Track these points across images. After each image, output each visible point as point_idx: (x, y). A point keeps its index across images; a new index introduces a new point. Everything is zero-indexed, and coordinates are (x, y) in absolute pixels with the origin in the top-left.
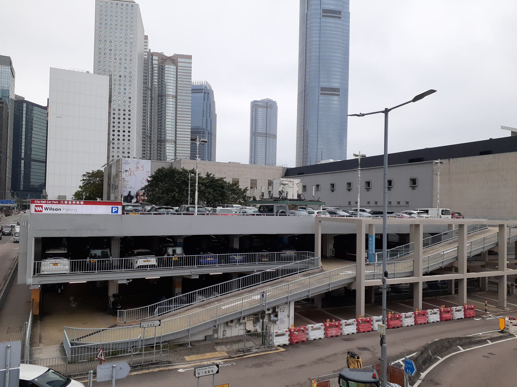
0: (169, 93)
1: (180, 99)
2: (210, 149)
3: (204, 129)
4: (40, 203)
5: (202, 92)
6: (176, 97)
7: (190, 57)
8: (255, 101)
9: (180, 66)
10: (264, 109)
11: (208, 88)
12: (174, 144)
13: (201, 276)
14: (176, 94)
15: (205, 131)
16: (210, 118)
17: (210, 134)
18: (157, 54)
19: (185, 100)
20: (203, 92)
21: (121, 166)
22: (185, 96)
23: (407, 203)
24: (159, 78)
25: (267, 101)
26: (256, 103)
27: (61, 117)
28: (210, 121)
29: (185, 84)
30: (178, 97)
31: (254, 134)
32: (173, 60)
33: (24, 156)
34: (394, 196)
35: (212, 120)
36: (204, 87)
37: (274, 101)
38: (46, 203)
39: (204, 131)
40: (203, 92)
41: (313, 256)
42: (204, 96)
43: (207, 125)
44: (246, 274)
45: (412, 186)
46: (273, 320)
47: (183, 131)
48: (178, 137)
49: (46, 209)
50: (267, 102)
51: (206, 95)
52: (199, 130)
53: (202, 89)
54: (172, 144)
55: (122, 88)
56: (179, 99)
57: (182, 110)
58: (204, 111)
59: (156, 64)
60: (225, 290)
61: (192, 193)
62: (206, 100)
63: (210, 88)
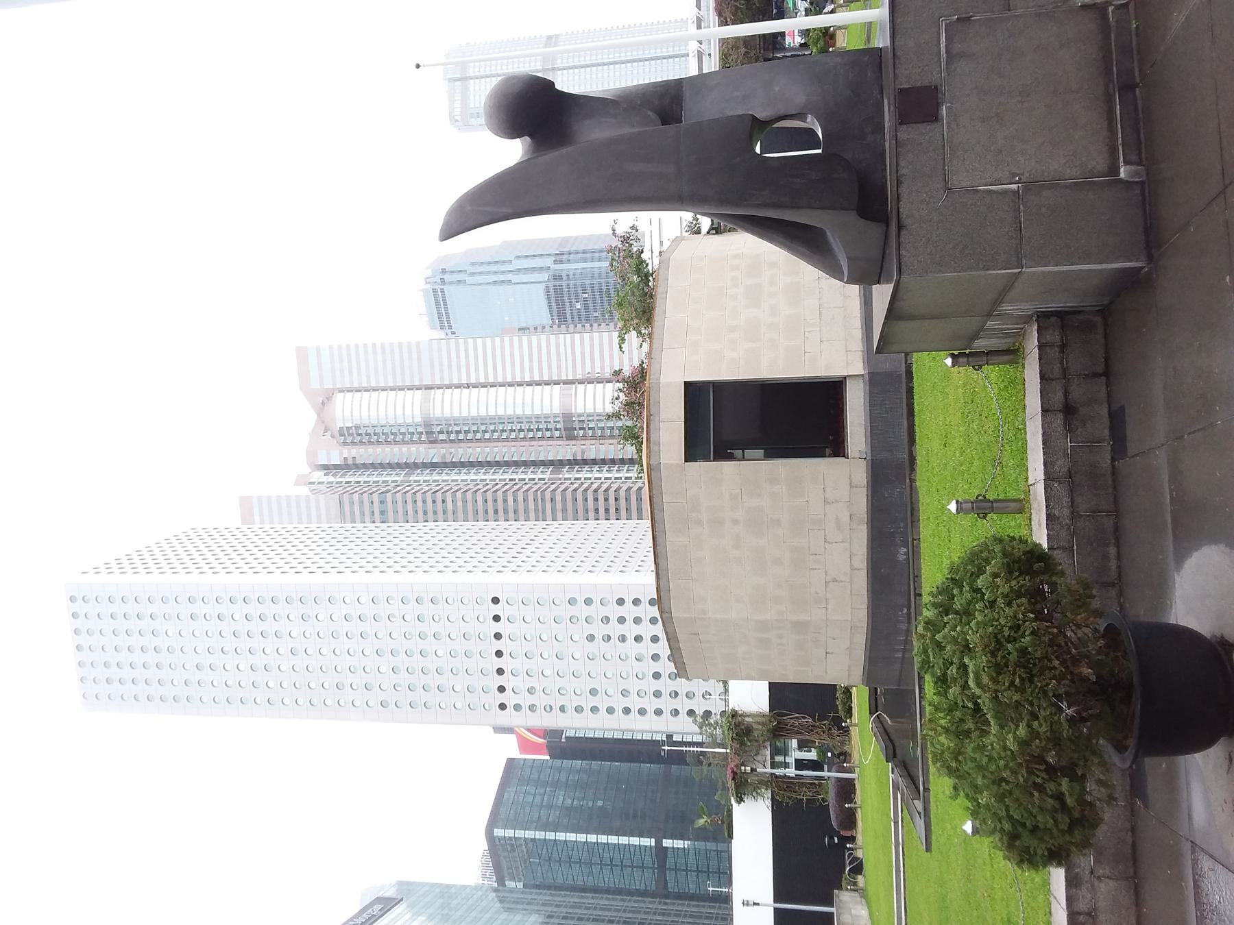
0: (417, 412)
1: (433, 375)
8: (453, 120)
10: (471, 88)
11: (429, 273)
12: (576, 389)
17: (559, 257)
18: (311, 454)
20: (442, 287)
22: (419, 359)
26: (458, 118)
29: (384, 362)
30: (428, 382)
33: (650, 837)
36: (428, 286)
40: (442, 287)
42: (451, 283)
47: (531, 360)
48: (550, 375)
50: (450, 80)
51: (447, 277)
52: (552, 291)
54: (576, 394)
55: (345, 627)
57: (464, 370)
58: (495, 282)
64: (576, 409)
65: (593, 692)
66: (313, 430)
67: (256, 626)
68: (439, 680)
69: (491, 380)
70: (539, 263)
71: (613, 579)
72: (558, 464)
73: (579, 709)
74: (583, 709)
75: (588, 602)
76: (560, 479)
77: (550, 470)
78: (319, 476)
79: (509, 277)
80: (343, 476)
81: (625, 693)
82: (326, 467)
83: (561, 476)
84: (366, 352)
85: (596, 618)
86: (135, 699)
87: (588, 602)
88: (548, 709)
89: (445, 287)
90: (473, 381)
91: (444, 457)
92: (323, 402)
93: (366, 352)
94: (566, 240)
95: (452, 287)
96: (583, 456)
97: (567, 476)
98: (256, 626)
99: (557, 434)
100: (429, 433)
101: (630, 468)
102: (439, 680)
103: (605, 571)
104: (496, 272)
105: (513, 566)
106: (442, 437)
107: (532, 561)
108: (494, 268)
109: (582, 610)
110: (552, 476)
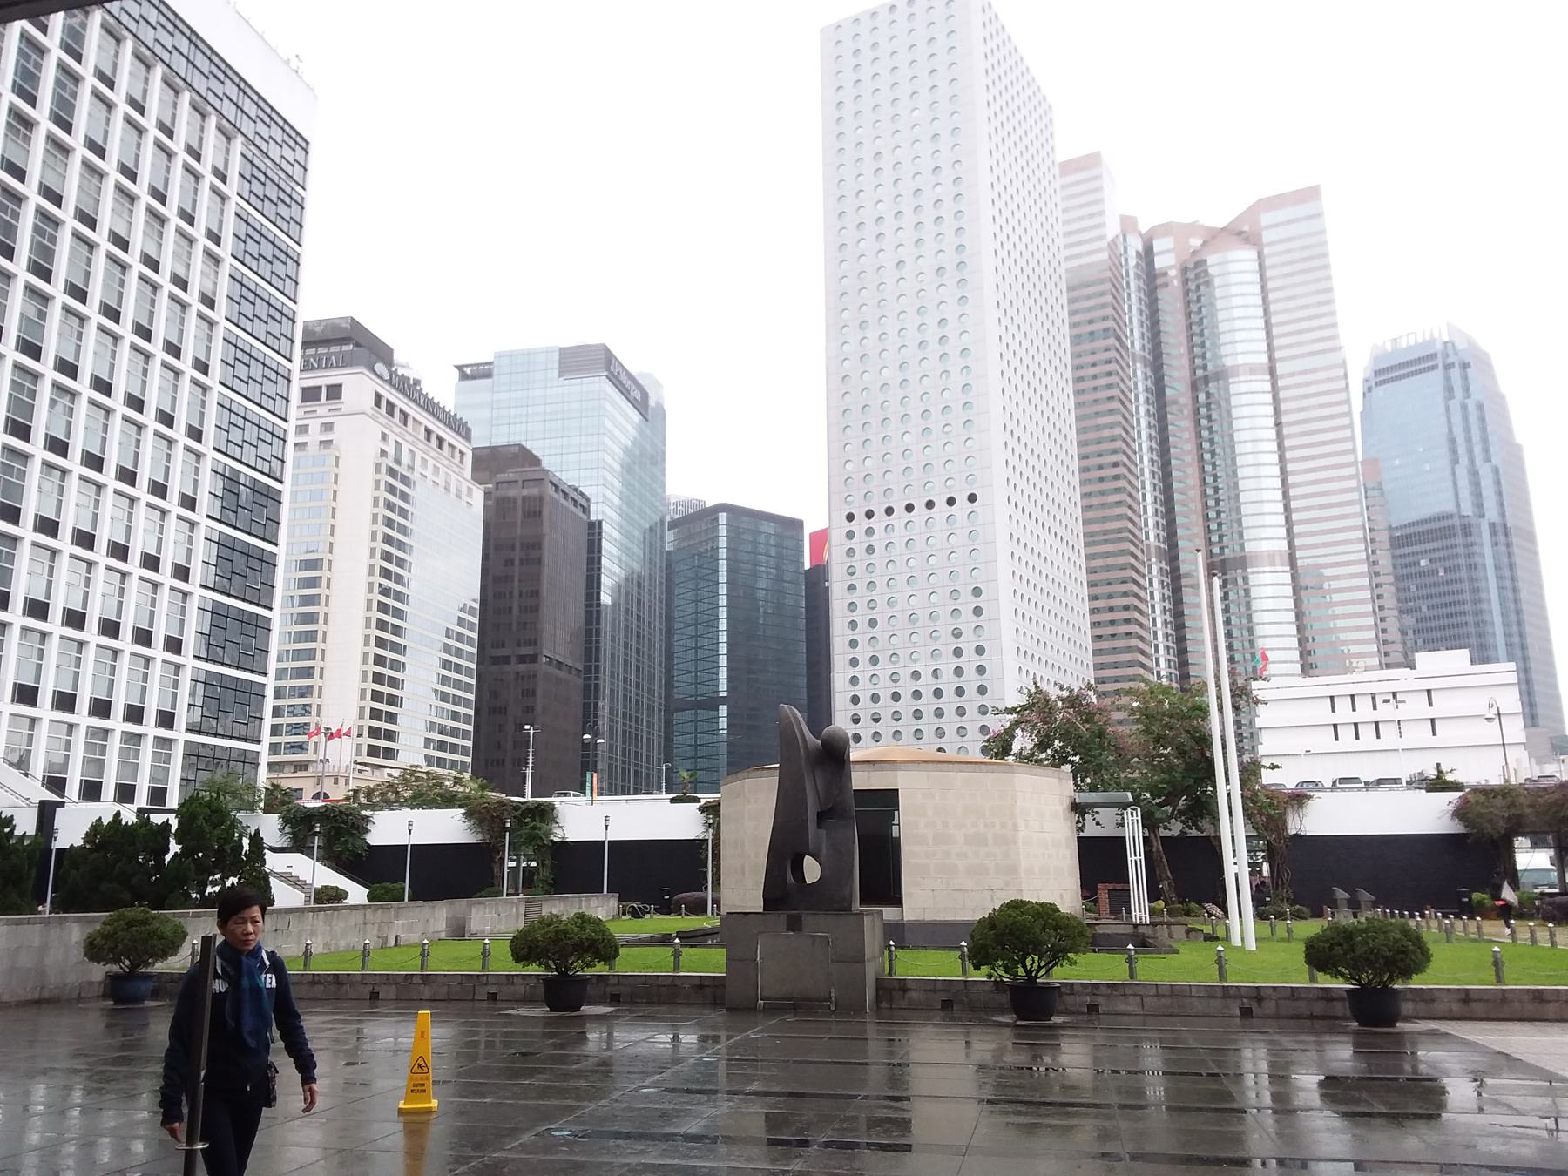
1: (1292, 375)
5: (1434, 367)
6: (1272, 371)
9: (1270, 244)
11: (1461, 346)
14: (1271, 358)
17: (1500, 529)
18: (1166, 229)
19: (1314, 371)
30: (1281, 368)
40: (1440, 366)
42: (1447, 378)
47: (1321, 507)
51: (1455, 373)
53: (1433, 356)
55: (932, 320)
56: (1283, 376)
62: (1459, 393)
63: (1473, 346)
64: (1253, 573)
65: (873, 623)
66: (1202, 226)
67: (928, 215)
68: (876, 439)
69: (1288, 455)
71: (1008, 641)
72: (1171, 555)
73: (852, 606)
74: (853, 611)
75: (978, 611)
76: (1149, 560)
77: (1162, 546)
78: (1136, 245)
79: (1464, 461)
80: (1138, 277)
81: (874, 660)
82: (1148, 254)
83: (1153, 560)
84: (1318, 281)
85: (959, 621)
86: (839, 88)
87: (978, 611)
88: (851, 571)
89: (1439, 373)
90: (1286, 431)
91: (1175, 402)
92: (1242, 233)
93: (1318, 281)
94: (1530, 537)
96: (1186, 586)
97: (1155, 569)
98: (928, 215)
99: (1216, 550)
100: (1206, 380)
101: (1171, 651)
102: (876, 439)
103: (1017, 629)
104: (1469, 440)
105: (1017, 515)
106: (1202, 397)
107: (1025, 538)
108: (1476, 437)
109: (967, 603)
110: (1153, 550)
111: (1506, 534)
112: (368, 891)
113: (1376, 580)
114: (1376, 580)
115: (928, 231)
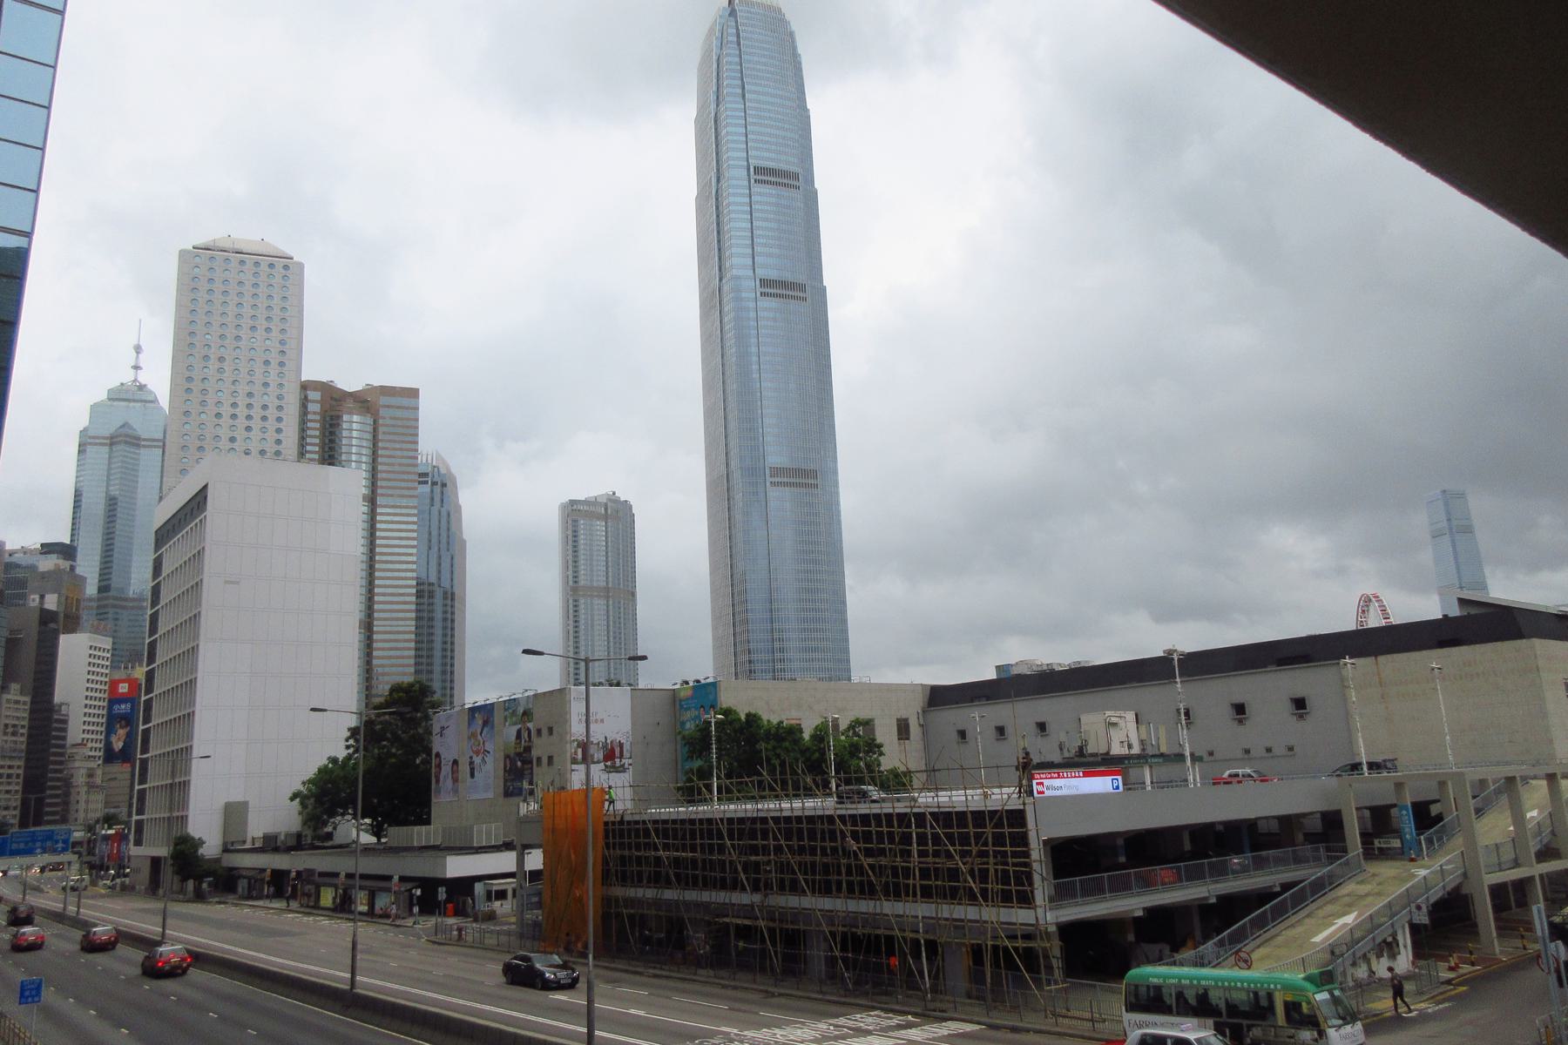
2: (449, 639)
3: (433, 584)
4: (1041, 778)
5: (426, 482)
7: (413, 393)
8: (573, 502)
11: (443, 471)
13: (1219, 897)
15: (436, 588)
16: (449, 553)
21: (568, 705)
23: (1291, 749)
24: (323, 449)
25: (605, 501)
26: (575, 507)
27: (238, 583)
28: (449, 560)
30: (380, 500)
31: (574, 591)
32: (366, 401)
34: (1253, 734)
35: (455, 560)
37: (622, 499)
38: (1046, 778)
39: (431, 588)
41: (1345, 851)
42: (432, 491)
43: (439, 572)
44: (1295, 882)
45: (1296, 714)
46: (1197, 1001)
49: (1048, 788)
50: (606, 505)
51: (438, 489)
58: (430, 534)
59: (315, 413)
60: (1280, 913)
61: (438, 769)
67: (257, 412)
70: (446, 575)
95: (429, 490)
98: (257, 412)
111: (453, 599)
112: (541, 850)
113: (419, 645)
114: (419, 645)
115: (256, 424)
